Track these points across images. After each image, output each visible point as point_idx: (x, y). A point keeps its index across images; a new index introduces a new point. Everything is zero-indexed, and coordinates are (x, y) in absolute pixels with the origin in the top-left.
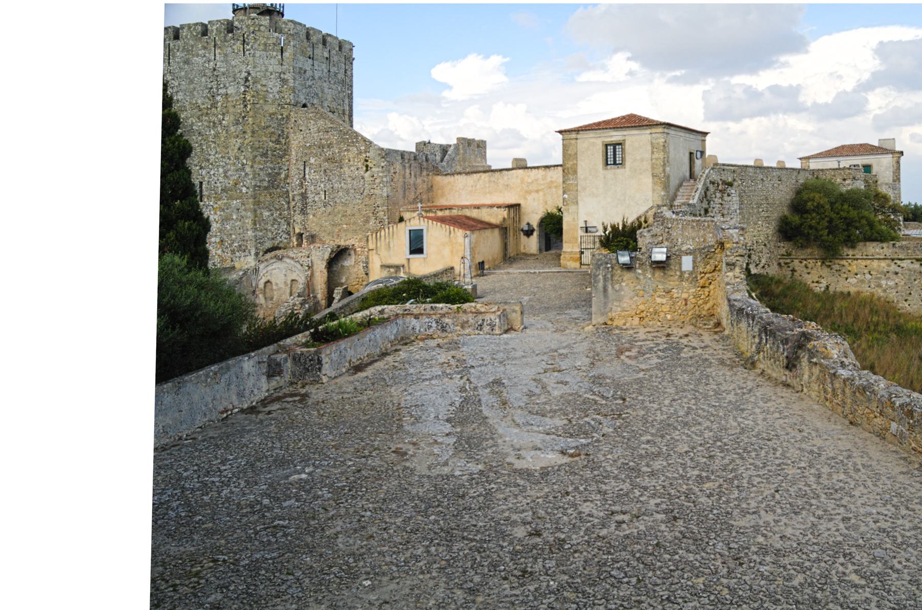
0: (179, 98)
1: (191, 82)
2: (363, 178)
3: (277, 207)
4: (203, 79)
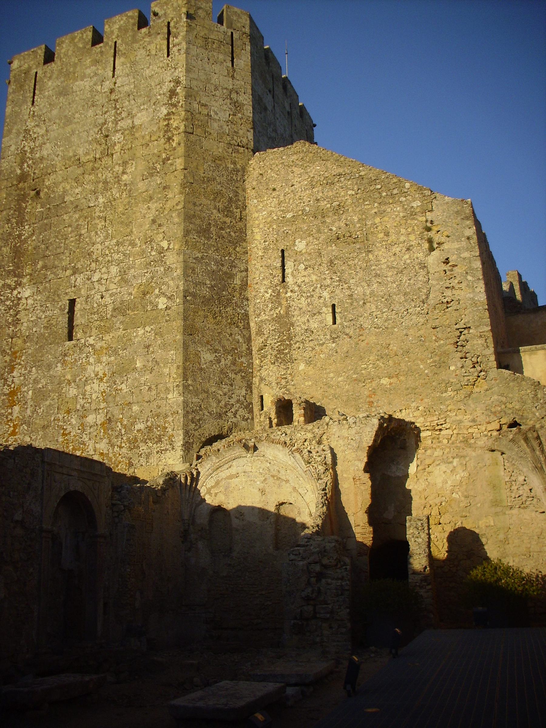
0: (45, 153)
1: (68, 121)
2: (424, 267)
3: (226, 343)
4: (90, 113)
